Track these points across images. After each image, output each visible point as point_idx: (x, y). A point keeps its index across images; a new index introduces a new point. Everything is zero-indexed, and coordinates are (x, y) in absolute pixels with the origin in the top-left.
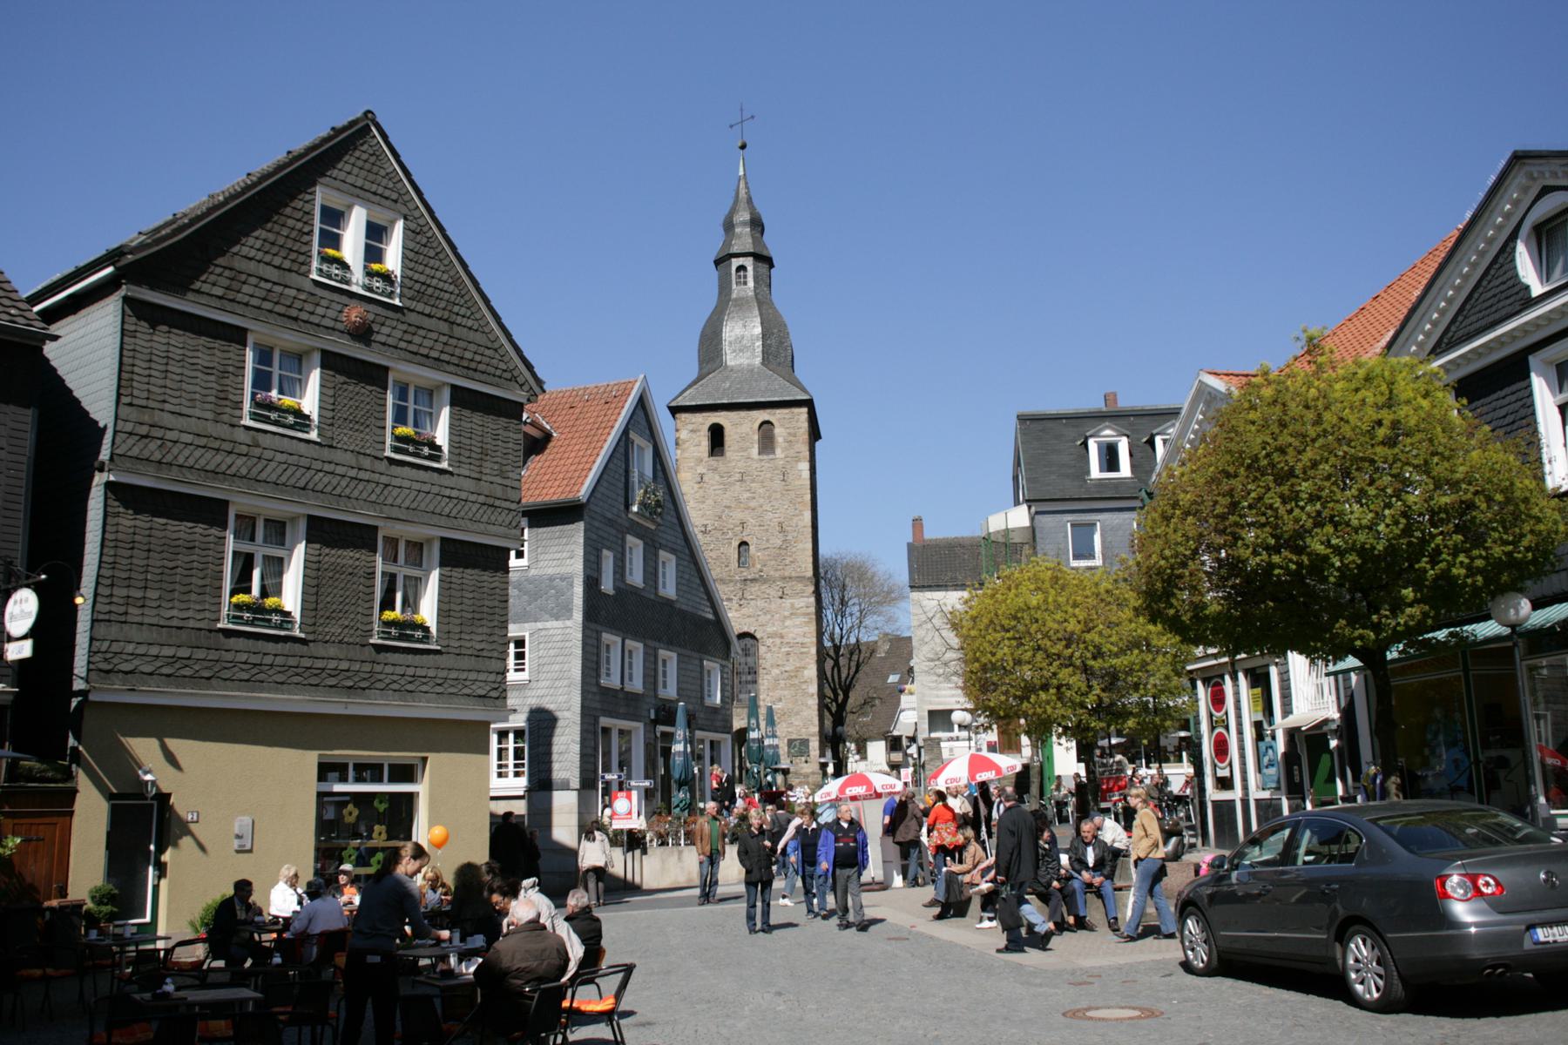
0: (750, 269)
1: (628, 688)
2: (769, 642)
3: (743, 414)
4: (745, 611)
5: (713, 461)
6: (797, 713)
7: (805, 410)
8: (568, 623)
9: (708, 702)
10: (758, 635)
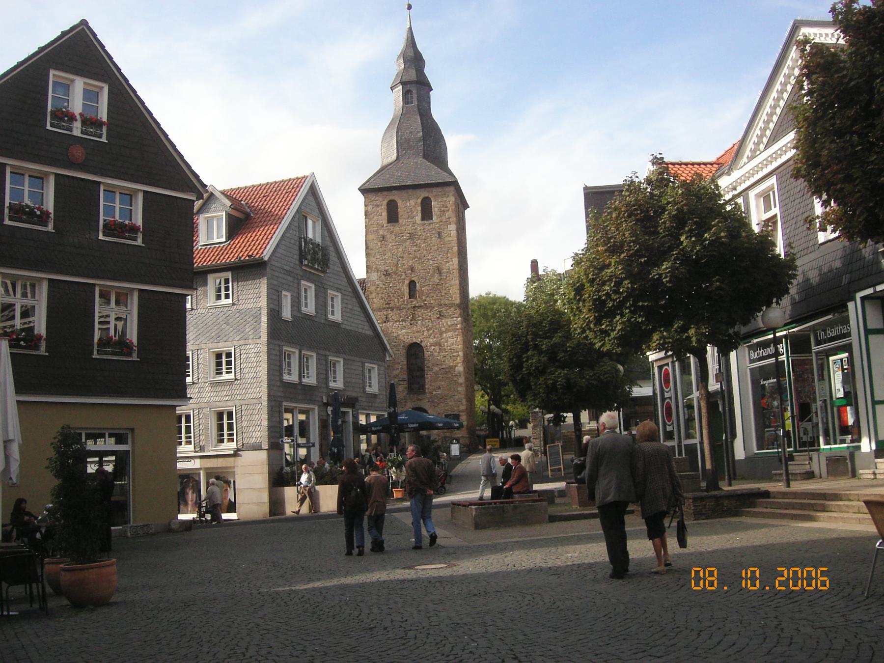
0: (414, 92)
1: (305, 380)
3: (410, 191)
4: (415, 328)
6: (451, 397)
8: (258, 341)
9: (368, 389)
10: (423, 344)
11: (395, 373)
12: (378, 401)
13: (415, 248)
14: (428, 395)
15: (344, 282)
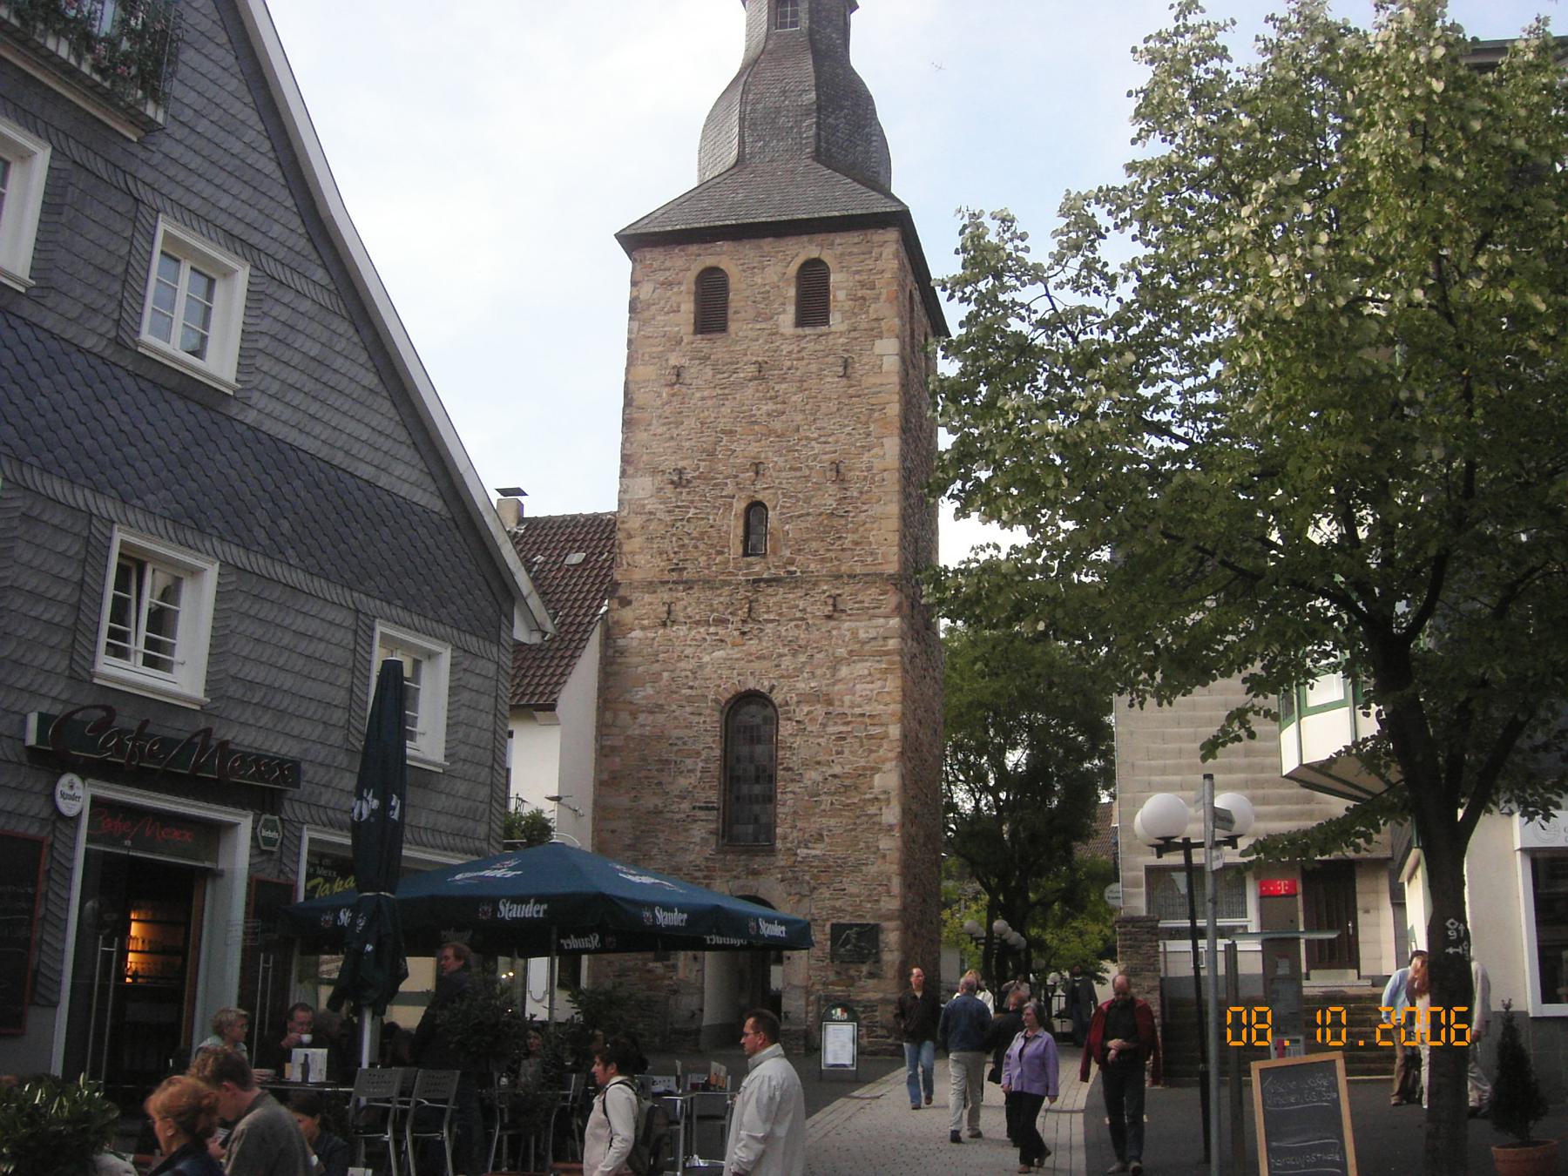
3: (768, 244)
5: (702, 343)
7: (892, 235)
10: (777, 698)
11: (683, 782)
12: (441, 802)
13: (770, 406)
14: (781, 860)
15: (286, 230)
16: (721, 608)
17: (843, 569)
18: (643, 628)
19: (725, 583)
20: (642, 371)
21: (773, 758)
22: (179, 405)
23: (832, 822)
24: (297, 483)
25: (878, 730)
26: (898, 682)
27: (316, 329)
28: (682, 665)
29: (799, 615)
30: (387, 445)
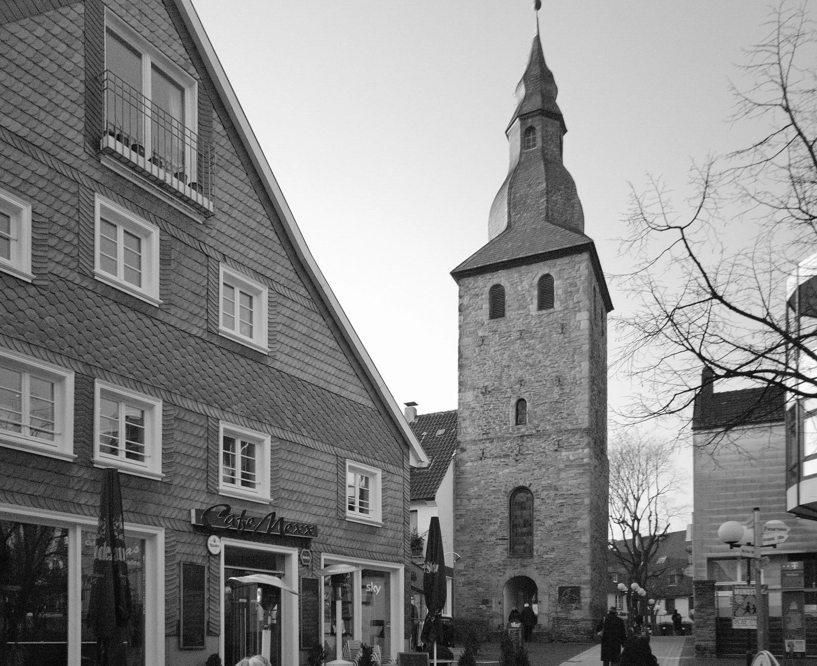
2: (544, 494)
4: (521, 466)
6: (570, 562)
10: (533, 489)
11: (492, 528)
14: (536, 560)
16: (506, 449)
17: (562, 427)
18: (472, 461)
19: (508, 438)
20: (467, 340)
21: (531, 515)
22: (242, 360)
23: (559, 542)
24: (303, 397)
25: (579, 500)
26: (588, 479)
27: (305, 320)
28: (490, 476)
29: (542, 450)
30: (343, 376)
